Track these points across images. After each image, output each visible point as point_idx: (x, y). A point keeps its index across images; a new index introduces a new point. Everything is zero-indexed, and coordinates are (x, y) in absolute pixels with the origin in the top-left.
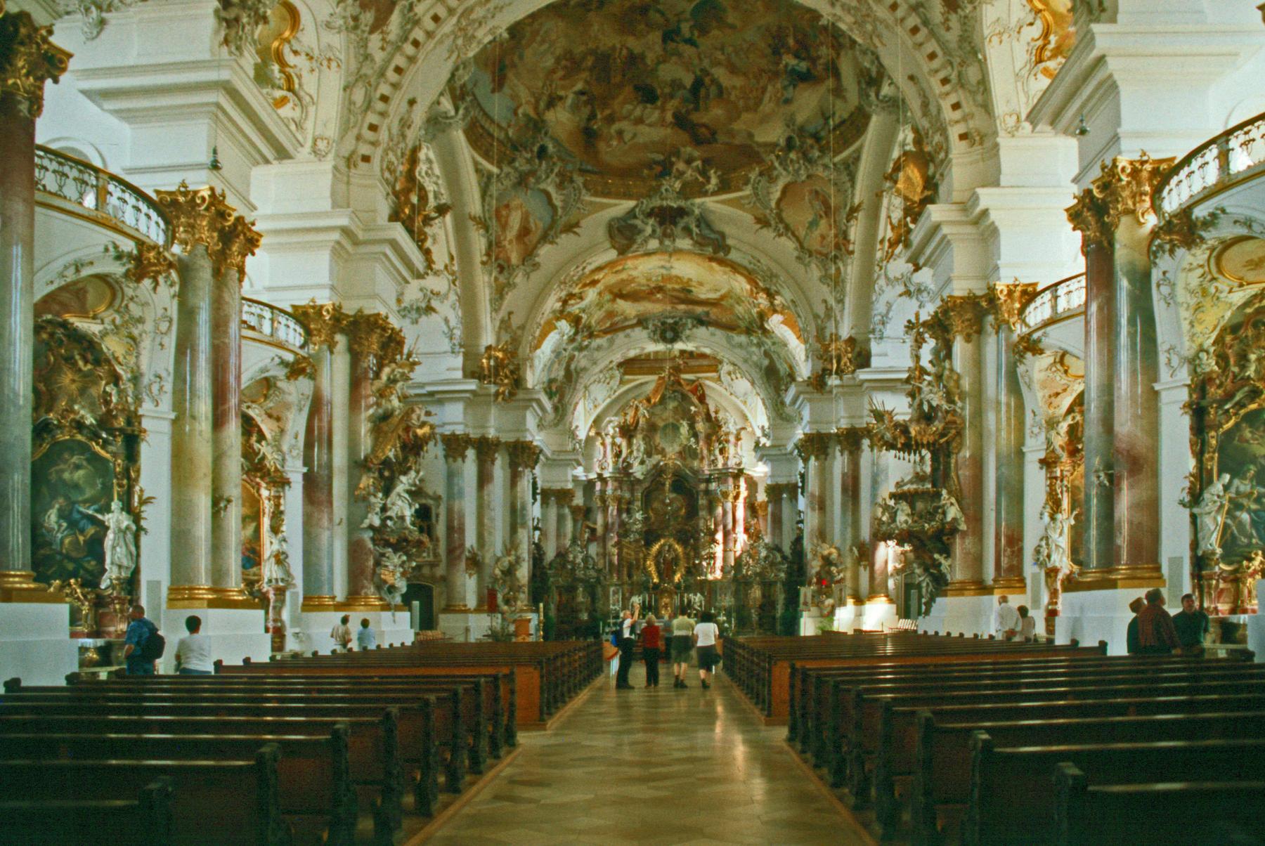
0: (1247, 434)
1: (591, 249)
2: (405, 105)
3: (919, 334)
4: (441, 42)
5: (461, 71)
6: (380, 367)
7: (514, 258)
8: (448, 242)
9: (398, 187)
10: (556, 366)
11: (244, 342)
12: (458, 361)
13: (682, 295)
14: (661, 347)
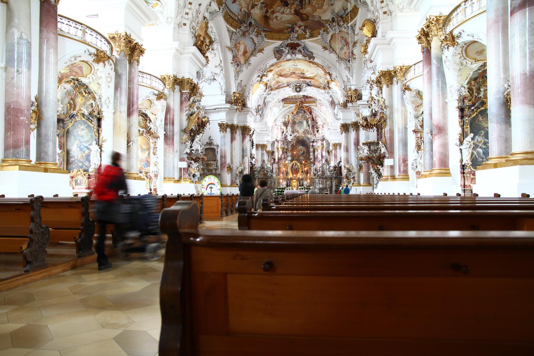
0: (481, 119)
2: (198, 6)
3: (371, 85)
7: (242, 61)
8: (219, 56)
9: (196, 35)
10: (260, 100)
11: (139, 86)
12: (224, 98)
13: (301, 75)
14: (296, 94)
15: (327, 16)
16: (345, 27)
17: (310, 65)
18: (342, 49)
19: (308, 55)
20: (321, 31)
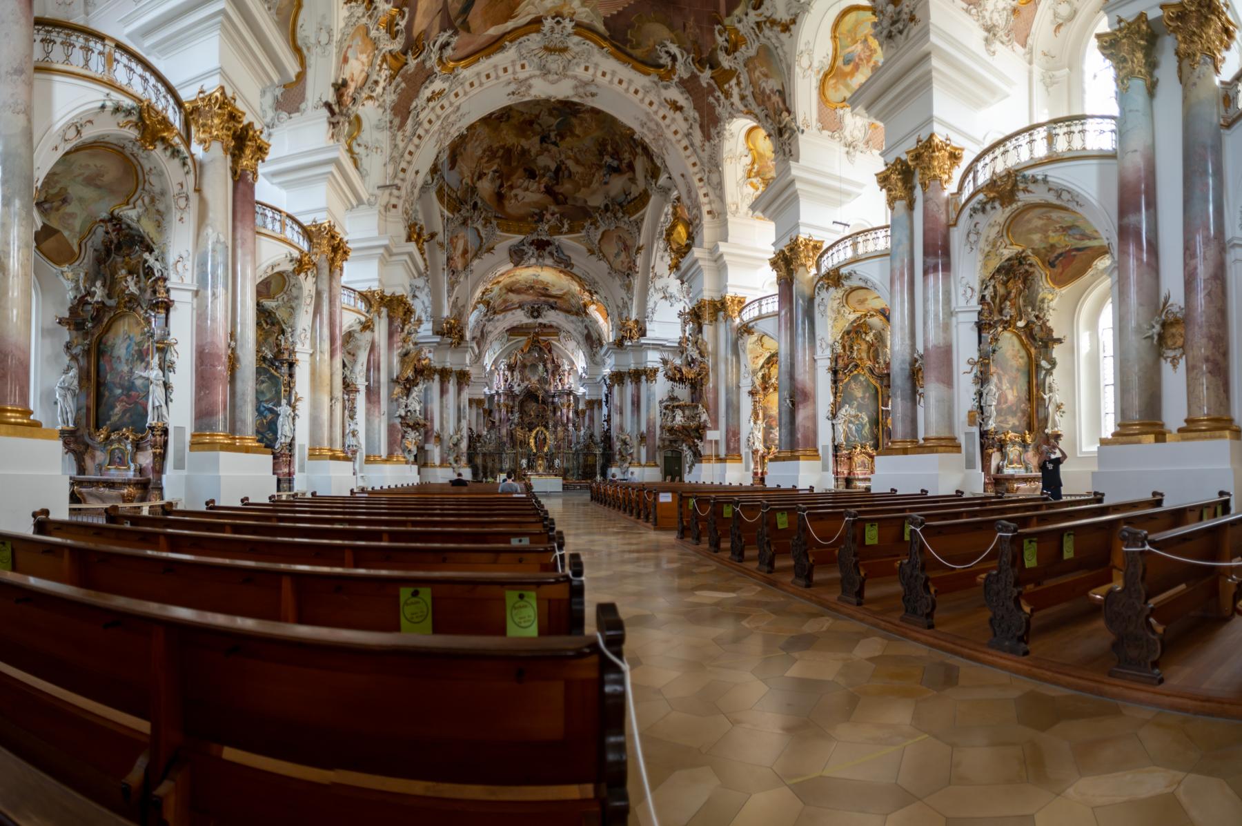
1: (500, 263)
4: (432, 135)
6: (404, 325)
14: (531, 320)
15: (597, 201)
16: (625, 222)
18: (617, 255)
20: (587, 224)
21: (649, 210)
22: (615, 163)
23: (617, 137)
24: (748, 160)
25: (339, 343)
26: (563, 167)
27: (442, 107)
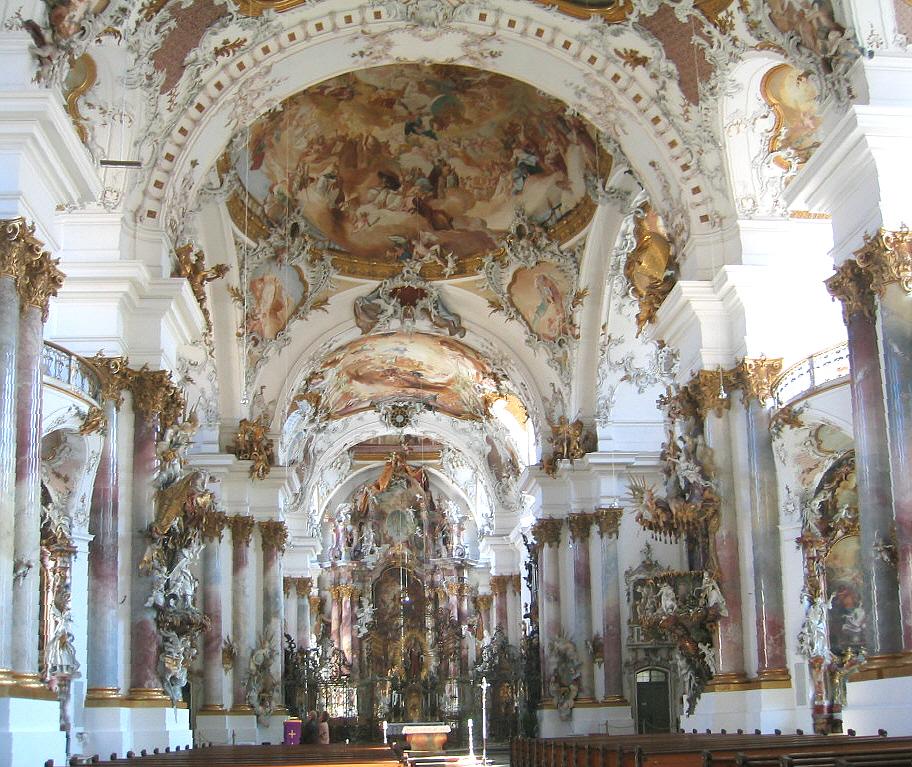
5: (238, 139)
13: (412, 379)
14: (392, 431)
15: (503, 220)
17: (442, 351)
18: (542, 308)
19: (448, 324)
20: (487, 261)
21: (594, 230)
22: (532, 160)
23: (534, 119)
24: (769, 123)
25: (34, 450)
26: (445, 170)
27: (241, 66)
